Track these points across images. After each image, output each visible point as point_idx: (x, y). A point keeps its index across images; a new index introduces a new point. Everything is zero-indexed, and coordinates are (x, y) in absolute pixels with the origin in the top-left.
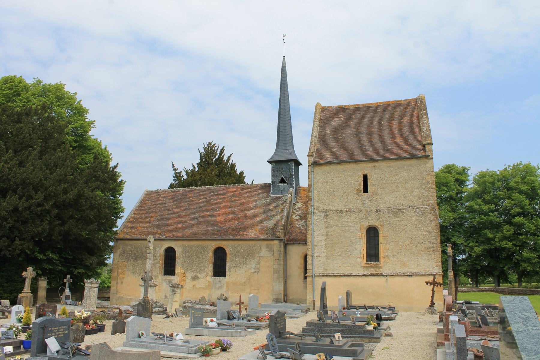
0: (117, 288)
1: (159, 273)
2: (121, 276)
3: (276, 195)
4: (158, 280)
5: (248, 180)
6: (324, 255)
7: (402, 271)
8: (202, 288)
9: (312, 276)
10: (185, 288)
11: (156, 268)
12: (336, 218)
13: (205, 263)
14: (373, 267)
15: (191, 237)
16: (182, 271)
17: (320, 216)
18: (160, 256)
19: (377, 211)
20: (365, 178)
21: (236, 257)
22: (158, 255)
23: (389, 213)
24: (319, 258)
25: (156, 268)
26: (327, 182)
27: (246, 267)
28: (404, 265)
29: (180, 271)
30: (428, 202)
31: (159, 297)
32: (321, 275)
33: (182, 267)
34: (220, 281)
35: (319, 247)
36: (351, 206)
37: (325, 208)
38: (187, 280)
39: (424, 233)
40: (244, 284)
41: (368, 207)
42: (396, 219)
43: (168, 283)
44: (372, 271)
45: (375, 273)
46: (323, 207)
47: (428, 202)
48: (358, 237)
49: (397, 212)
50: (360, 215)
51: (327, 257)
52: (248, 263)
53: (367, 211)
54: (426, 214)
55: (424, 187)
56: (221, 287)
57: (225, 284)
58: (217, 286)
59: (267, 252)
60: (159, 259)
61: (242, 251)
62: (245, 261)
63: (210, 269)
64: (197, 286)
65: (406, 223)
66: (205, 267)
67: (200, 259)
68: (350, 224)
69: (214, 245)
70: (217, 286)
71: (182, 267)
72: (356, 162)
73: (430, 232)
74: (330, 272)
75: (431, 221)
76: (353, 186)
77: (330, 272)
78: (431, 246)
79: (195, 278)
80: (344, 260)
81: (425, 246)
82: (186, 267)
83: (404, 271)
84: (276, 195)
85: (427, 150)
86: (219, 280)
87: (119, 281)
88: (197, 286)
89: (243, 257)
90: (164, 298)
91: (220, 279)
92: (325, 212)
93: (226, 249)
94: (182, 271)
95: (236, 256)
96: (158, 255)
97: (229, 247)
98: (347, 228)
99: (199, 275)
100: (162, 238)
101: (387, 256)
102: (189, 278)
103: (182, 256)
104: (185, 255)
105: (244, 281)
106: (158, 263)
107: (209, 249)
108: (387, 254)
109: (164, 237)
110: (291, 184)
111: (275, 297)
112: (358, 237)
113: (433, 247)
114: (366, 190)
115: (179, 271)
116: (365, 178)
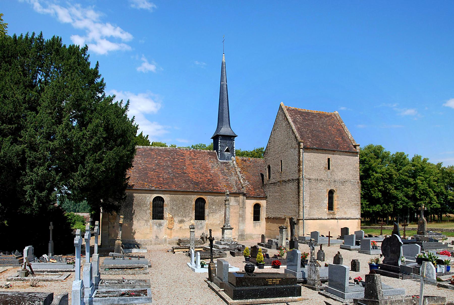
0: (109, 231)
1: (149, 218)
2: (112, 221)
3: (223, 161)
4: (149, 224)
5: (151, 140)
6: (308, 206)
7: (344, 216)
8: (187, 228)
9: (303, 219)
10: (174, 230)
11: (146, 214)
12: (315, 183)
13: (189, 209)
14: (332, 214)
15: (178, 189)
16: (170, 216)
17: (306, 181)
18: (150, 204)
19: (334, 182)
20: (329, 159)
21: (213, 205)
22: (148, 203)
23: (340, 183)
24: (306, 208)
25: (146, 214)
26: (310, 161)
27: (220, 212)
28: (345, 213)
29: (169, 216)
30: (356, 179)
31: (150, 238)
32: (307, 218)
33: (171, 213)
34: (201, 224)
35: (306, 201)
36: (322, 177)
37: (309, 177)
38: (175, 223)
39: (354, 195)
40: (219, 225)
41: (330, 179)
42: (343, 187)
43: (159, 226)
44: (331, 216)
45: (333, 217)
46: (308, 176)
47: (356, 179)
48: (325, 196)
49: (343, 182)
50: (327, 183)
51: (310, 207)
52: (221, 210)
53: (330, 181)
54: (356, 185)
55: (354, 169)
56: (202, 228)
57: (205, 226)
58: (199, 227)
59: (235, 202)
60: (149, 206)
61: (217, 201)
62: (220, 208)
63: (193, 215)
64: (183, 228)
65: (347, 189)
66: (189, 212)
67: (185, 207)
68: (322, 188)
69: (195, 197)
70: (199, 227)
71: (171, 213)
72: (325, 150)
73: (357, 195)
74: (312, 217)
75: (357, 189)
76: (323, 164)
77: (311, 217)
78: (357, 203)
79: (181, 222)
80: (318, 209)
81: (354, 203)
82: (174, 213)
83: (345, 216)
84: (223, 161)
85: (357, 149)
86: (200, 222)
87: (110, 225)
88: (183, 228)
89: (218, 206)
90: (155, 238)
91: (201, 222)
92: (309, 179)
93: (206, 200)
94: (170, 216)
95: (213, 204)
96: (148, 203)
97: (207, 198)
98: (320, 190)
99: (185, 219)
100: (152, 189)
101: (338, 208)
102: (177, 221)
103: (170, 204)
104: (173, 204)
105: (219, 223)
106: (148, 210)
107: (193, 199)
108: (338, 207)
109: (154, 188)
110: (232, 154)
111: (240, 233)
112: (325, 196)
113: (358, 204)
114: (329, 169)
115: (168, 216)
116: (329, 159)
